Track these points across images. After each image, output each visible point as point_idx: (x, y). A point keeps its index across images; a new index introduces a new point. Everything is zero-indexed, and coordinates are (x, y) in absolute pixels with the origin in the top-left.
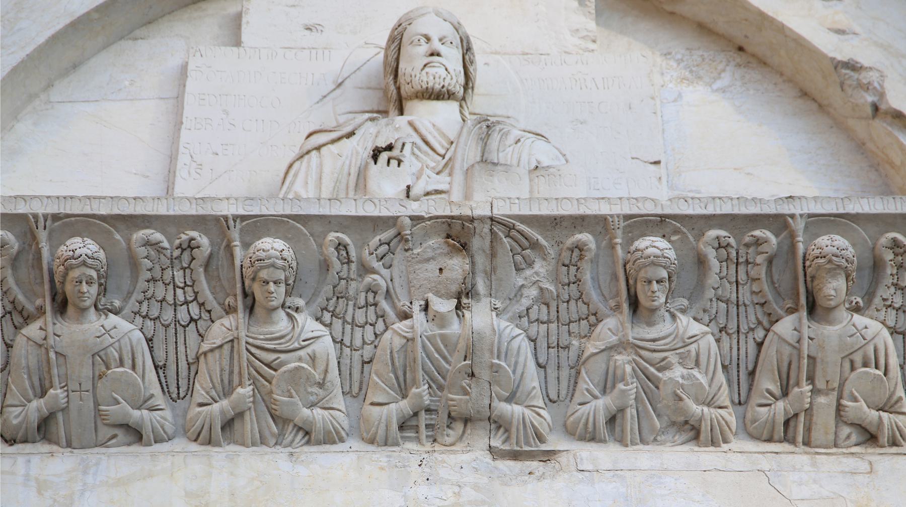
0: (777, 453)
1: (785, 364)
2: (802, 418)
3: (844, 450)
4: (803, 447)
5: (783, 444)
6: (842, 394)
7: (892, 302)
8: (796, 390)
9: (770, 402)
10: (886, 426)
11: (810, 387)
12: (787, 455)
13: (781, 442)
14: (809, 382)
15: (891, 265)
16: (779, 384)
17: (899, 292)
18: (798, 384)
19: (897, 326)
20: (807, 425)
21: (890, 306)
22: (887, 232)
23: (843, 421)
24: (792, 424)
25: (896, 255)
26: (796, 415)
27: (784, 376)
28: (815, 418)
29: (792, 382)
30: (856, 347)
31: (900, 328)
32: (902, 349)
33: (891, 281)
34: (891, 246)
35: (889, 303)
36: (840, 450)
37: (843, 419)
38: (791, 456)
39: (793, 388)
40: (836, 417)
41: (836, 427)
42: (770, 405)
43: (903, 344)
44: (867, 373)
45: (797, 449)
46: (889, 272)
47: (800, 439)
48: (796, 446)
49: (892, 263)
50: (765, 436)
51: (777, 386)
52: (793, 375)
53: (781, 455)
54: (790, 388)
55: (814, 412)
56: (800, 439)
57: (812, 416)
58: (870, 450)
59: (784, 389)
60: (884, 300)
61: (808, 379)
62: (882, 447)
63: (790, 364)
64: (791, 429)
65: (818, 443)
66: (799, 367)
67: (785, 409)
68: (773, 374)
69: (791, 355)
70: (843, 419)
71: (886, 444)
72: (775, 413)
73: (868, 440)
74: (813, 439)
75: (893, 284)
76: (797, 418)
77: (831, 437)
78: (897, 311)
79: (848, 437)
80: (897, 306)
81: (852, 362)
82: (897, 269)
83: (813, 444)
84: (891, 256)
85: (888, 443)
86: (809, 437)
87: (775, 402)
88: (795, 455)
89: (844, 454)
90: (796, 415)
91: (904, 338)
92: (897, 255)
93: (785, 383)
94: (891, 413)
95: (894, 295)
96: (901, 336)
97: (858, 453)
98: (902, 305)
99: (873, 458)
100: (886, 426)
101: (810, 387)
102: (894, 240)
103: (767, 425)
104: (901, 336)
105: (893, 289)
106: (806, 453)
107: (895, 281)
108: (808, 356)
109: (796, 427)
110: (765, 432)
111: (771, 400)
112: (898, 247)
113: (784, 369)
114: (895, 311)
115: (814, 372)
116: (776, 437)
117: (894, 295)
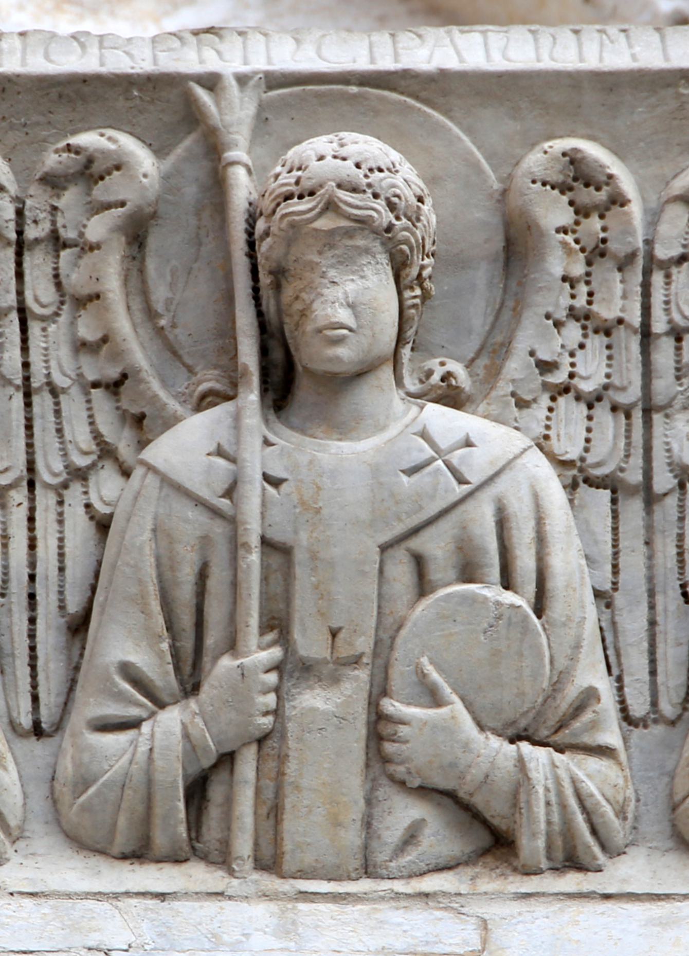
0: (162, 896)
1: (187, 575)
2: (247, 766)
3: (399, 886)
4: (256, 876)
5: (185, 867)
6: (386, 678)
7: (572, 376)
8: (226, 662)
9: (134, 712)
10: (541, 790)
11: (276, 653)
12: (197, 904)
13: (177, 860)
14: (270, 637)
15: (564, 244)
16: (165, 646)
17: (596, 342)
18: (232, 645)
19: (591, 459)
20: (269, 794)
21: (566, 390)
22: (550, 138)
23: (392, 779)
24: (216, 792)
25: (582, 212)
26: (227, 759)
27: (186, 620)
28: (292, 768)
29: (212, 639)
30: (433, 509)
31: (598, 465)
32: (609, 537)
33: (565, 301)
34: (560, 178)
35: (559, 377)
36: (386, 885)
37: (391, 768)
38: (211, 907)
39: (216, 659)
40: (367, 766)
41: (369, 802)
42: (133, 724)
43: (609, 522)
44: (472, 600)
45: (235, 882)
46: (558, 270)
47: (243, 845)
48: (231, 872)
49: (569, 239)
50: (122, 841)
51: (160, 654)
52: (215, 613)
53: (176, 904)
54: (206, 659)
55: (291, 743)
56: (243, 845)
57: (282, 759)
58: (488, 884)
59: (187, 669)
60: (546, 367)
61: (265, 628)
62: (529, 872)
63: (202, 576)
64: (214, 813)
65: (308, 859)
66: (235, 585)
67: (186, 736)
68: (145, 611)
69: (205, 541)
70: (391, 768)
71: (544, 864)
72: (151, 750)
73: (485, 852)
74: (288, 846)
75: (573, 313)
76: (232, 771)
77: (352, 837)
78: (590, 406)
79: (411, 837)
80: (587, 387)
81: (419, 562)
82: (589, 263)
83: (289, 864)
84: (566, 216)
85: (549, 858)
86: (277, 840)
87: (152, 714)
88: (227, 904)
89: (397, 896)
90: (227, 759)
91: (614, 501)
92: (587, 216)
93: (187, 644)
94: (560, 750)
95: (579, 353)
96: (606, 494)
97: (445, 894)
98: (606, 387)
99: (493, 911)
100: (541, 790)
101: (276, 653)
102: (573, 159)
103: (128, 792)
104: (606, 494)
105: (573, 332)
106: (266, 896)
107: (581, 302)
108: (266, 542)
109: (229, 802)
110: (122, 821)
111: (141, 705)
112: (587, 185)
113: (185, 593)
114: (583, 408)
115: (288, 599)
116: (160, 840)
117: (579, 353)
